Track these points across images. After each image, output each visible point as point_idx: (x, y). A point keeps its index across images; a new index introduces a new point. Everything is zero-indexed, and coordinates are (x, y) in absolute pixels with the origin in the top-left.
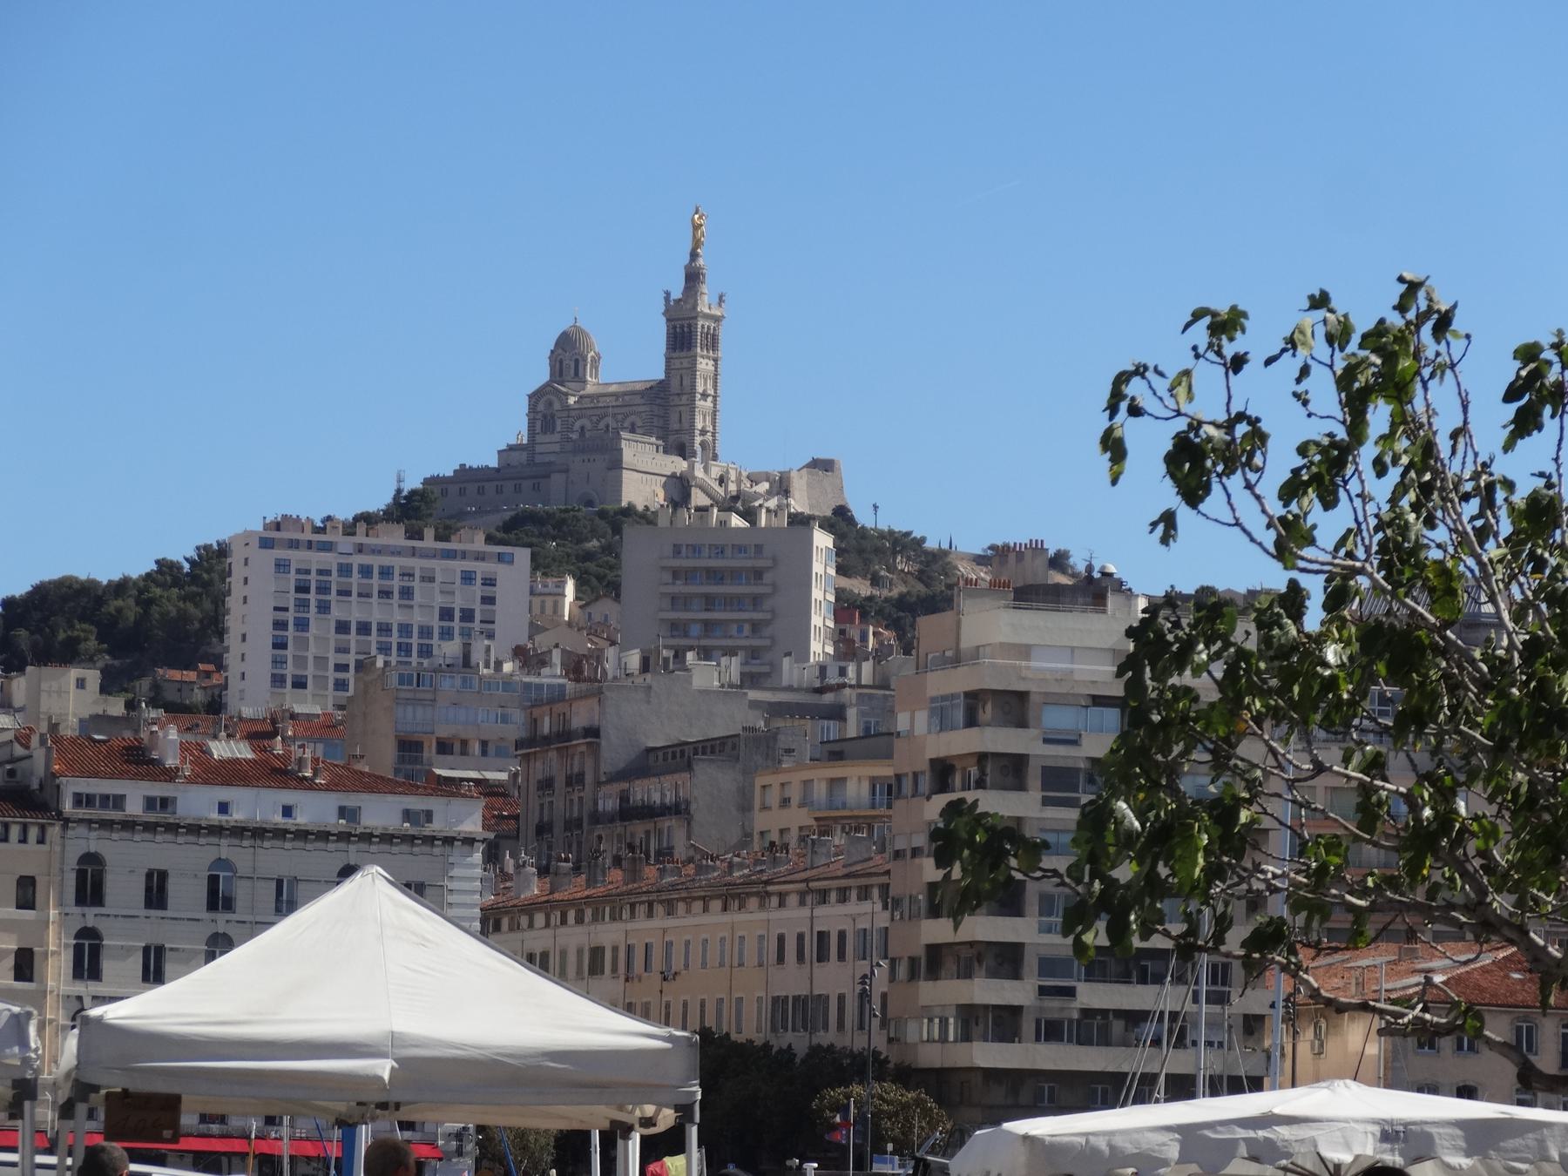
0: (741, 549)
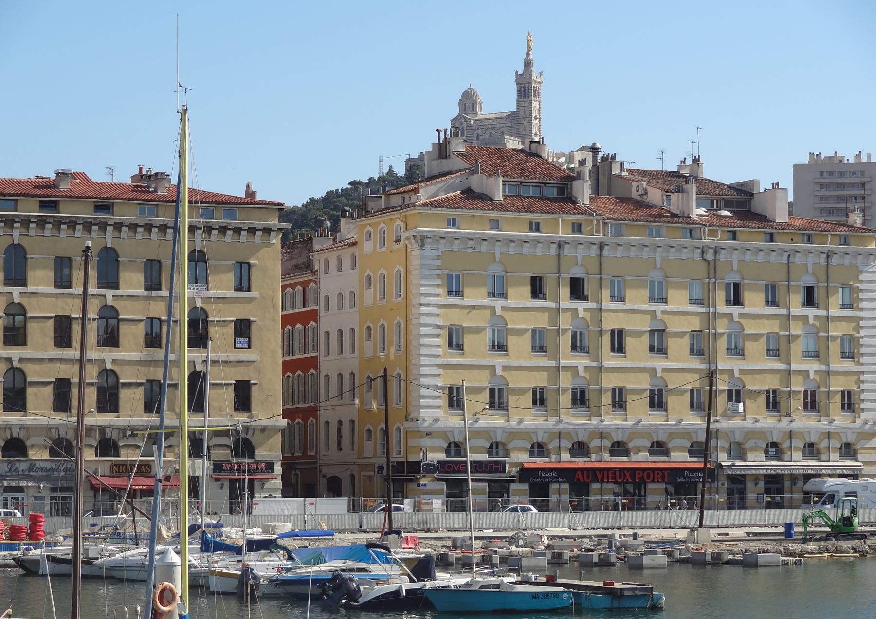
0: (854, 173)
